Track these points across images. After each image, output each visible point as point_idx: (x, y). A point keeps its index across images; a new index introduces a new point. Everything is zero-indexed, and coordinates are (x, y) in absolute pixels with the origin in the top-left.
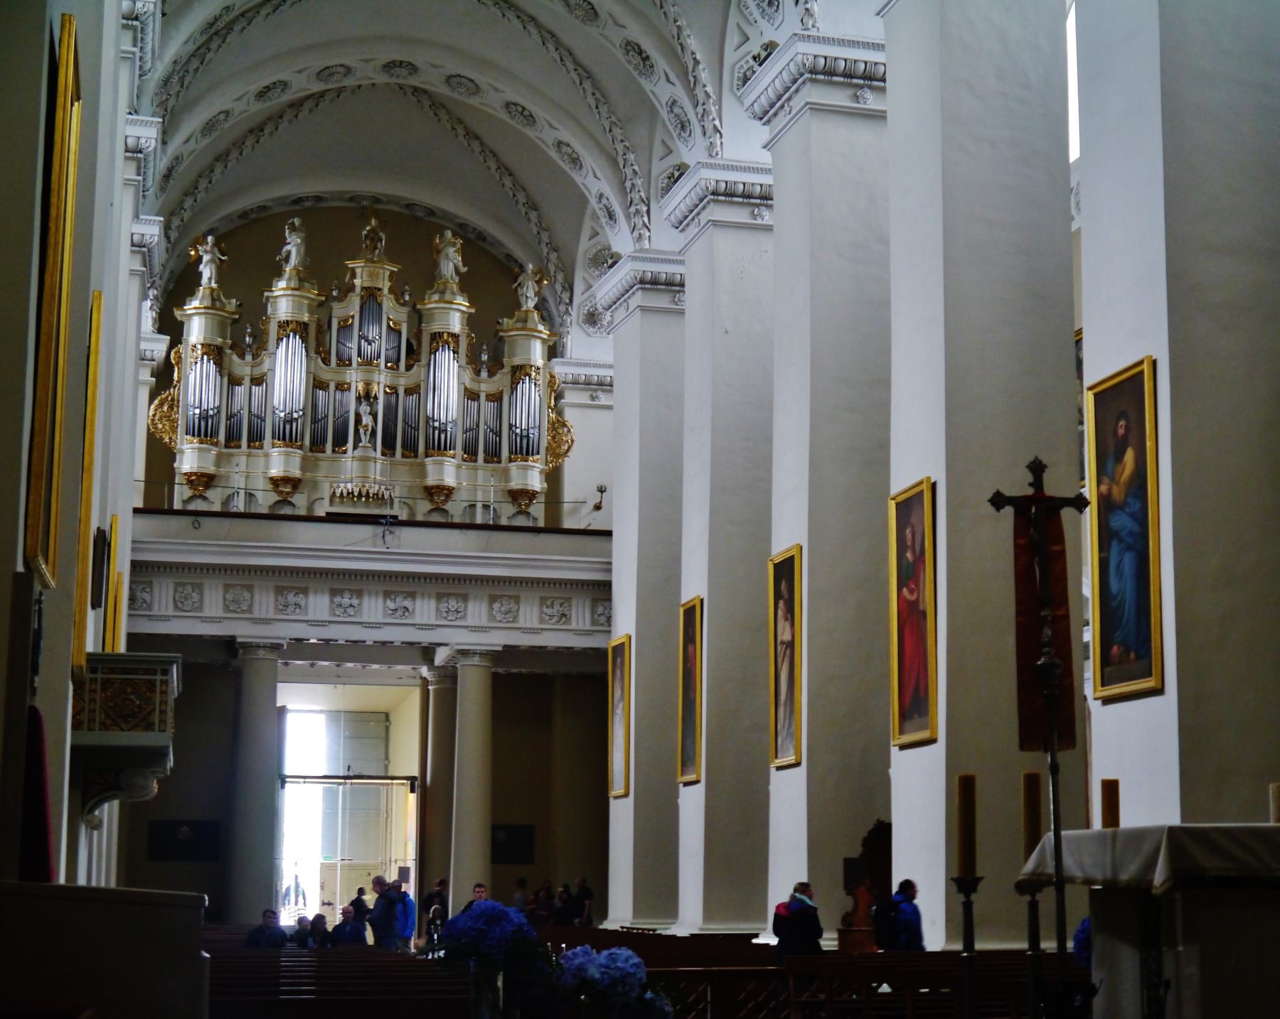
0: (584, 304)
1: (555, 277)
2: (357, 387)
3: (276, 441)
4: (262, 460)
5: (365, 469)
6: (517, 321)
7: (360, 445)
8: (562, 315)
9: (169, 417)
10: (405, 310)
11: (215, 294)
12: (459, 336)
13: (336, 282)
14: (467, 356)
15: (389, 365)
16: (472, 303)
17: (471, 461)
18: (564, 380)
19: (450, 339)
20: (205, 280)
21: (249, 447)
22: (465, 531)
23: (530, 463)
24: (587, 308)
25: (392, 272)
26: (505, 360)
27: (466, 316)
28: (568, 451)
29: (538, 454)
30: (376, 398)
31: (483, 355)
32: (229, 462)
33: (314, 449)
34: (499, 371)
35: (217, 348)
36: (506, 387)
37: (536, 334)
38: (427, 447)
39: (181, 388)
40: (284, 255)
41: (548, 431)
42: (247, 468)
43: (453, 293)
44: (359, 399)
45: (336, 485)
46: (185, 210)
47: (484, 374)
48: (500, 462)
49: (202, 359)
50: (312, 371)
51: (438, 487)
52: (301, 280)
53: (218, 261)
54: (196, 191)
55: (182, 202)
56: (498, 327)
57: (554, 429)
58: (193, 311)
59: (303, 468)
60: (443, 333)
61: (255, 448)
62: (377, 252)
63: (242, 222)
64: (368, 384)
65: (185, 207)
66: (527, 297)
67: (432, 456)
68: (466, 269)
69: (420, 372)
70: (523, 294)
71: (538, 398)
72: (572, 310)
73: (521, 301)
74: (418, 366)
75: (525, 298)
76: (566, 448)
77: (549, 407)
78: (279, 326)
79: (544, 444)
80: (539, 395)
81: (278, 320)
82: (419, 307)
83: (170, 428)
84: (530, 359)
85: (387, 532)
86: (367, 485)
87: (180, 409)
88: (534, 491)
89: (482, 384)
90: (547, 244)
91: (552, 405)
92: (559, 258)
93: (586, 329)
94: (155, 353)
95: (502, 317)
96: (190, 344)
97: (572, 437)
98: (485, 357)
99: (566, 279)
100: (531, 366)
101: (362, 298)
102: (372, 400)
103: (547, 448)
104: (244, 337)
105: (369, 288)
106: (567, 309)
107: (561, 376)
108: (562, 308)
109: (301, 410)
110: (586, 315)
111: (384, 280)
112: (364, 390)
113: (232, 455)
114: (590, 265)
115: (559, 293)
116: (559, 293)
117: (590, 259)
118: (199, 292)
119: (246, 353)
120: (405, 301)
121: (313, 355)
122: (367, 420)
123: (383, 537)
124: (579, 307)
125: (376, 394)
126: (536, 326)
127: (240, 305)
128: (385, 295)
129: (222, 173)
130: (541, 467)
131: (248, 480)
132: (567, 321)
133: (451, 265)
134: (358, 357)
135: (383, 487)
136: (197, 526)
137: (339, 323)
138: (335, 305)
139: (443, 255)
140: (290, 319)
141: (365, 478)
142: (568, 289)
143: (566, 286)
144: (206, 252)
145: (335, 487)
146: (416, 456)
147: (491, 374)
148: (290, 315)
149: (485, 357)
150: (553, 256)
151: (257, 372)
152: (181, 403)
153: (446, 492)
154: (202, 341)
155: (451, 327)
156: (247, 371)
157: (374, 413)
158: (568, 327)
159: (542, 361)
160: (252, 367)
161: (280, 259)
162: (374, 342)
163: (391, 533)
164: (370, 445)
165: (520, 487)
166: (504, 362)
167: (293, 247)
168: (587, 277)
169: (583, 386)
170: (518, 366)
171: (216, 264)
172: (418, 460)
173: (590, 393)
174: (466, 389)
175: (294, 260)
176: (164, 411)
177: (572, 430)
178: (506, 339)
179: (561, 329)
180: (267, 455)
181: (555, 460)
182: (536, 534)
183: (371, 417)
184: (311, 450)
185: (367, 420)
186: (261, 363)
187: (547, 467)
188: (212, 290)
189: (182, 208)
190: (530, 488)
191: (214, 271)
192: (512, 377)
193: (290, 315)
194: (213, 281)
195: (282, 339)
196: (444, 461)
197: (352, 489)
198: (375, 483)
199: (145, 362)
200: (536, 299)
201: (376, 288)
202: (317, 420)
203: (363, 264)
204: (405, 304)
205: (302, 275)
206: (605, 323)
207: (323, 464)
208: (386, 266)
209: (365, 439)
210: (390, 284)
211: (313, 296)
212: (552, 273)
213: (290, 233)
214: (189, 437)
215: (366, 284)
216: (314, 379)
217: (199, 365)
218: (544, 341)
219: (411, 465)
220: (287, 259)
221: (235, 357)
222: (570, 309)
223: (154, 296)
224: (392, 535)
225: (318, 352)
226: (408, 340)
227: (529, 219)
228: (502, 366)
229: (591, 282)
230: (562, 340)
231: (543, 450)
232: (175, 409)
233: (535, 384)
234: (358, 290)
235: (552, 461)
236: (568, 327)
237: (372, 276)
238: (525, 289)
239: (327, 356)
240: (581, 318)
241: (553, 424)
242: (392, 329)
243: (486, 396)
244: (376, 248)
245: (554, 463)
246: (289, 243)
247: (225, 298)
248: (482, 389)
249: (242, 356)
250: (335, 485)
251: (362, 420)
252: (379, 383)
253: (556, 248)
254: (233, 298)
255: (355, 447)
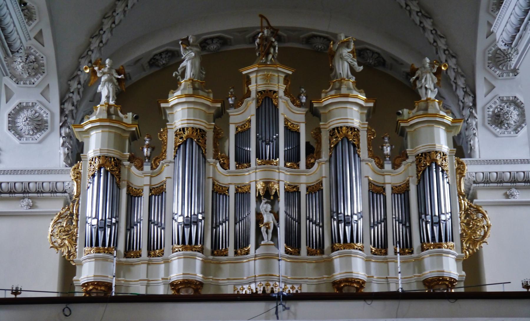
0: (488, 106)
1: (456, 83)
2: (256, 187)
3: (176, 246)
4: (162, 266)
5: (268, 267)
6: (417, 111)
7: (262, 243)
8: (466, 119)
9: (68, 231)
10: (303, 111)
11: (112, 110)
12: (358, 130)
13: (232, 90)
14: (369, 150)
15: (289, 164)
16: (369, 97)
17: (381, 254)
18: (475, 179)
19: (350, 133)
20: (104, 100)
21: (149, 255)
22: (369, 302)
23: (444, 249)
24: (491, 110)
25: (287, 76)
26: (409, 150)
27: (366, 112)
28: (484, 236)
29: (453, 241)
30: (276, 196)
31: (385, 147)
32: (129, 271)
33: (216, 252)
34: (404, 162)
35: (114, 160)
36: (412, 177)
37: (438, 119)
38: (332, 242)
39: (80, 203)
40: (180, 71)
41: (460, 218)
42: (147, 277)
43: (349, 89)
44: (259, 199)
45: (241, 287)
46: (92, 52)
47: (388, 166)
48: (412, 252)
49: (99, 171)
50: (211, 176)
51: (347, 280)
52: (194, 89)
53: (115, 81)
54: (102, 32)
55: (90, 44)
56: (399, 118)
57: (467, 215)
58: (90, 126)
59: (205, 271)
60: (341, 127)
61: (155, 255)
62: (270, 57)
63: (155, 69)
64: (267, 183)
65: (92, 48)
66: (426, 88)
67: (338, 250)
68: (361, 68)
69: (321, 171)
70: (422, 87)
71: (447, 186)
72: (476, 112)
73: (420, 94)
74: (318, 163)
75: (424, 90)
76: (482, 234)
77: (460, 194)
78: (176, 135)
79: (458, 230)
80: (448, 183)
81: (175, 130)
82: (315, 105)
83: (69, 242)
84: (435, 145)
85: (280, 307)
86: (271, 283)
87: (79, 222)
88: (451, 278)
89: (386, 177)
90: (444, 51)
91: (463, 191)
92: (457, 64)
93: (493, 130)
94: (66, 184)
95: (402, 109)
96: (89, 159)
97: (487, 222)
98: (387, 150)
99: (467, 84)
100: (437, 152)
101: (257, 102)
102: (272, 197)
103: (461, 235)
104: (143, 150)
105: (264, 91)
106: (471, 113)
107: (471, 175)
108: (466, 112)
109: (200, 213)
110: (492, 117)
111: (279, 82)
112: (263, 189)
113: (132, 265)
114: (491, 65)
115: (461, 98)
116: (461, 98)
117: (489, 59)
118: (97, 110)
119: (144, 163)
120: (302, 103)
121: (211, 160)
122: (268, 218)
123: (277, 313)
124: (483, 109)
125: (276, 192)
126: (439, 112)
127: (136, 118)
128: (281, 97)
129: (125, 11)
130: (457, 254)
131: (149, 288)
132: (472, 123)
133: (346, 64)
134: (257, 157)
135: (289, 286)
136: (68, 315)
137: (237, 128)
138: (231, 111)
139: (337, 58)
140: (185, 126)
141: (268, 276)
142: (470, 93)
143: (468, 90)
144: (104, 74)
145: (239, 290)
146: (322, 253)
147: (395, 166)
148: (186, 122)
149: (387, 150)
150: (452, 62)
151: (156, 181)
152: (79, 216)
153: (356, 285)
154: (99, 154)
155: (349, 121)
156: (147, 181)
157: (276, 212)
158: (474, 129)
159: (447, 147)
160: (151, 177)
161: (176, 75)
162: (272, 141)
163: (286, 308)
164: (272, 243)
165: (435, 275)
166: (408, 152)
167: (187, 61)
168: (488, 78)
169: (496, 184)
170: (422, 154)
171: (114, 83)
172: (324, 256)
173: (504, 192)
174: (370, 183)
175: (189, 74)
176: (63, 226)
177: (487, 216)
178: (408, 130)
179: (467, 133)
180: (167, 262)
181: (471, 247)
182: (452, 301)
183: (272, 215)
184: (213, 254)
185: (268, 217)
186: (159, 174)
187: (464, 254)
188: (110, 106)
189: (90, 50)
190: (446, 275)
191: (111, 90)
192: (417, 165)
193: (186, 122)
194: (111, 99)
195: (179, 146)
196: (351, 253)
197: (256, 289)
198: (279, 282)
199: (58, 194)
200: (436, 90)
201: (271, 91)
202: (218, 224)
203: (256, 69)
204: (301, 105)
205: (196, 85)
206: (512, 123)
207: (226, 268)
208: (279, 69)
209: (267, 238)
210: (285, 86)
211: (208, 103)
212: (453, 79)
213: (185, 49)
214: (87, 249)
215: (260, 89)
216: (214, 184)
217: (96, 178)
218: (448, 128)
219: (317, 262)
220: (183, 76)
221: (133, 169)
222: (474, 112)
223: (66, 133)
224: (286, 311)
225: (216, 157)
226: (307, 144)
227: (424, 28)
228: (407, 157)
229: (493, 83)
230: (469, 143)
231: (457, 238)
232: (74, 223)
233: (443, 171)
234: (253, 95)
235: (468, 248)
236: (474, 129)
237: (267, 79)
238: (423, 81)
239: (226, 161)
240: (487, 119)
241: (466, 210)
242: (290, 130)
243: (392, 189)
244: (267, 54)
245: (471, 251)
246: (184, 60)
247: (121, 112)
248: (386, 182)
249: (140, 167)
250: (239, 287)
251: (263, 219)
252: (279, 181)
253: (454, 55)
254: (130, 112)
255: (257, 246)
